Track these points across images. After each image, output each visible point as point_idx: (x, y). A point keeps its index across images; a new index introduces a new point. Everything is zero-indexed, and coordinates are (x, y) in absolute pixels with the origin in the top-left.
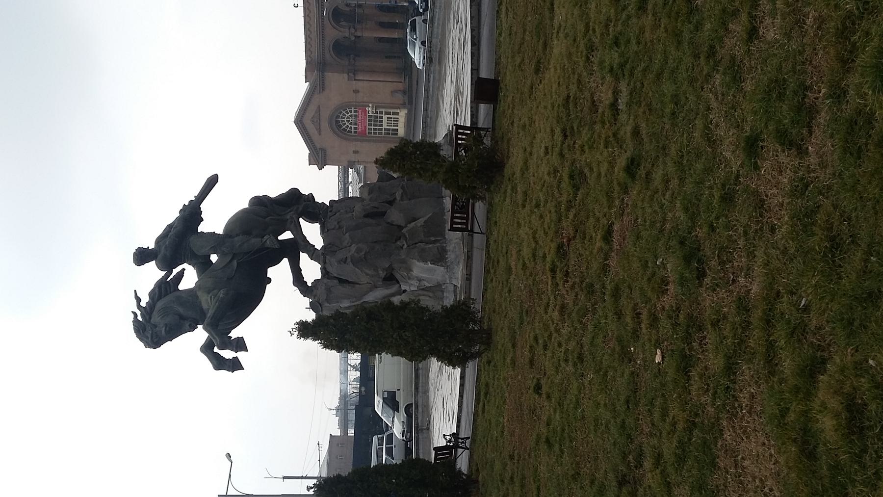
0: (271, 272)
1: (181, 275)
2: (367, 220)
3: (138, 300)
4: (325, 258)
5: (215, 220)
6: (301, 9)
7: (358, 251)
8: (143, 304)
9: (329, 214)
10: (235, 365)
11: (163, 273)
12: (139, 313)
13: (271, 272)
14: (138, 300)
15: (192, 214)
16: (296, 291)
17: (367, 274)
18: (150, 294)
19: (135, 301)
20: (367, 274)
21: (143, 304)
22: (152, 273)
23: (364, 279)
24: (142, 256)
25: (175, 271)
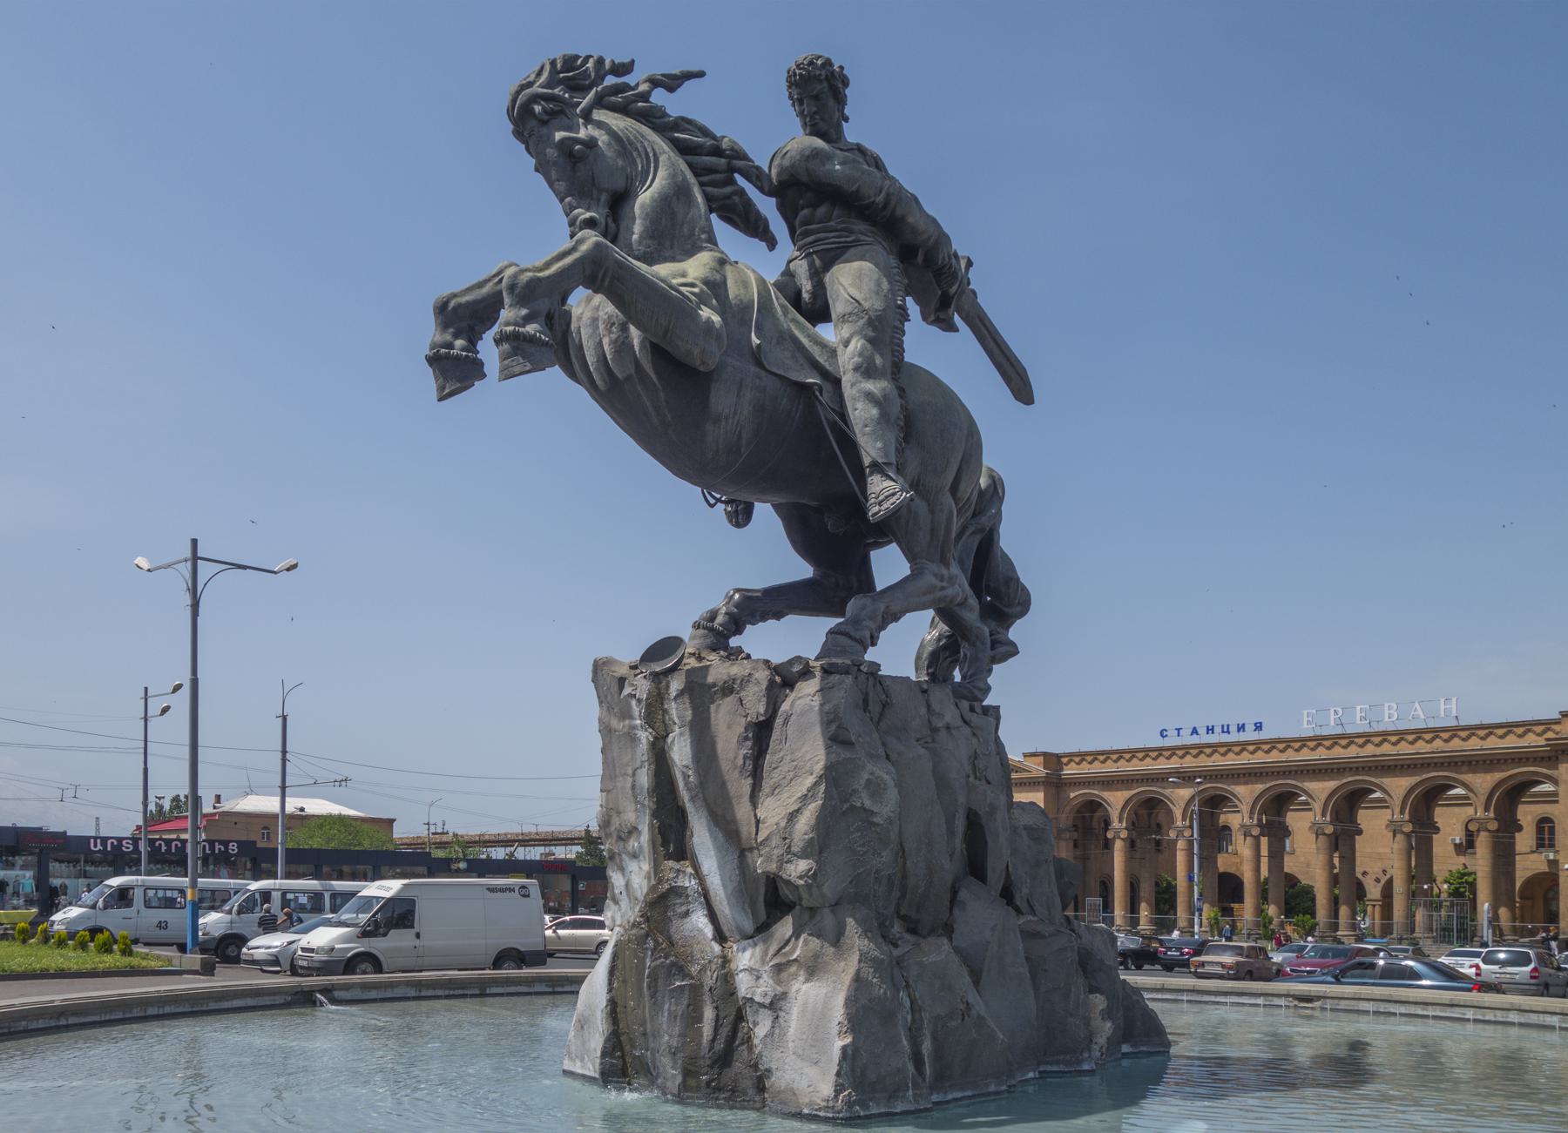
2: (960, 824)
4: (845, 671)
7: (876, 789)
9: (965, 704)
11: (761, 158)
17: (792, 817)
20: (792, 817)
23: (772, 811)
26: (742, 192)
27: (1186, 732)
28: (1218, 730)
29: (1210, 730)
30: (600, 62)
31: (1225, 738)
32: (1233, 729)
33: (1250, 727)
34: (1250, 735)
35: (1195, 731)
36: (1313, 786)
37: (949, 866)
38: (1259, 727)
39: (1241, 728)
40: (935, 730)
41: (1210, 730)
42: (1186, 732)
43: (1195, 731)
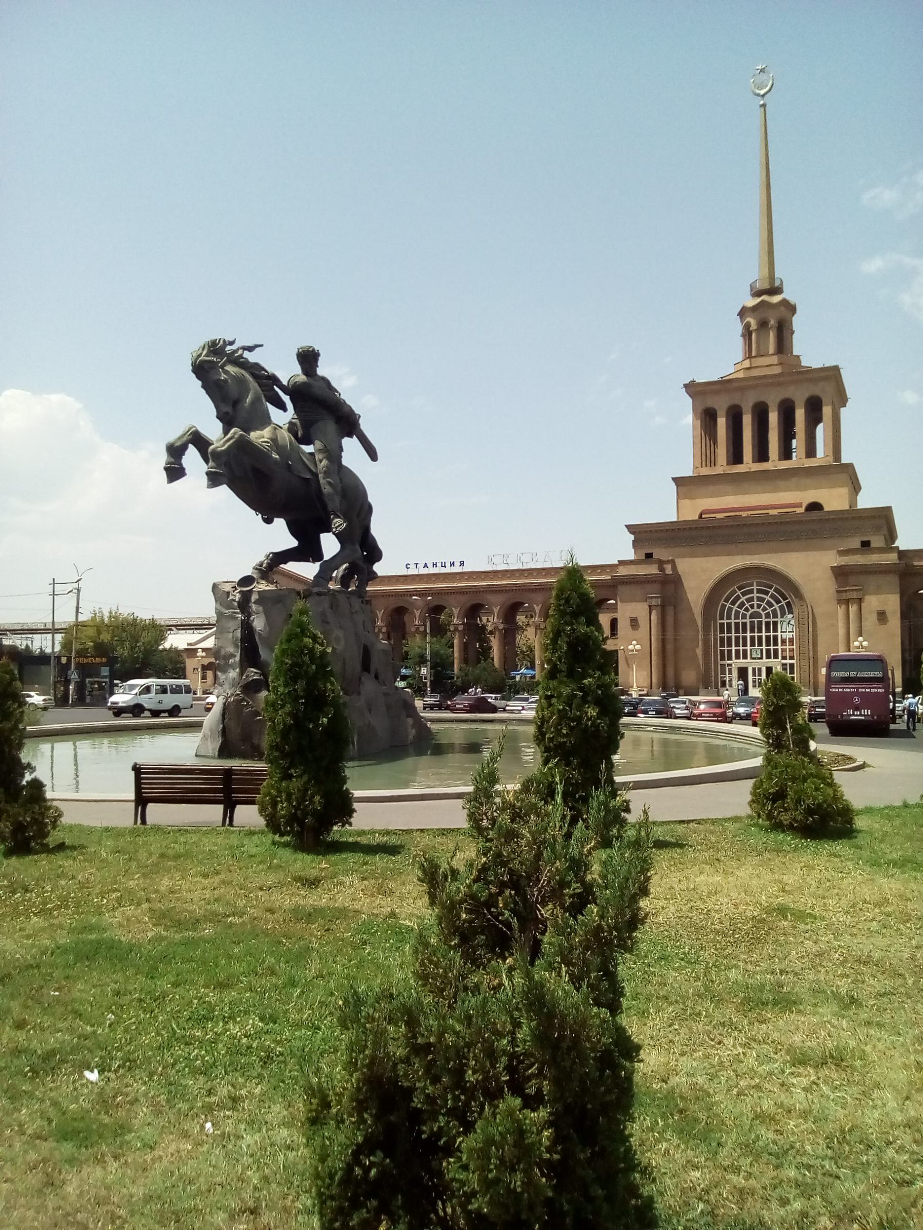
0: (280, 523)
1: (282, 406)
3: (250, 349)
5: (351, 453)
6: (405, 572)
8: (246, 354)
10: (175, 472)
11: (285, 383)
12: (234, 347)
13: (280, 523)
14: (250, 349)
15: (348, 423)
16: (260, 556)
18: (257, 366)
19: (251, 344)
21: (246, 354)
22: (287, 370)
24: (308, 359)
25: (286, 399)
26: (277, 393)
27: (421, 566)
28: (439, 565)
29: (435, 565)
30: (224, 341)
31: (443, 570)
32: (448, 565)
33: (457, 564)
34: (457, 569)
35: (426, 566)
36: (491, 598)
37: (358, 666)
38: (462, 564)
39: (452, 564)
40: (352, 613)
41: (435, 565)
42: (421, 566)
43: (426, 566)
